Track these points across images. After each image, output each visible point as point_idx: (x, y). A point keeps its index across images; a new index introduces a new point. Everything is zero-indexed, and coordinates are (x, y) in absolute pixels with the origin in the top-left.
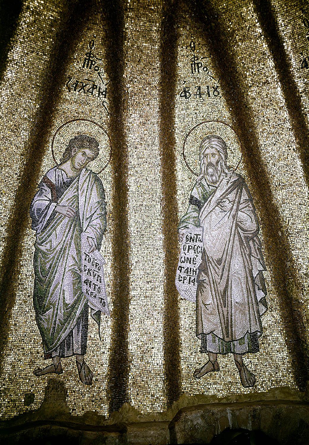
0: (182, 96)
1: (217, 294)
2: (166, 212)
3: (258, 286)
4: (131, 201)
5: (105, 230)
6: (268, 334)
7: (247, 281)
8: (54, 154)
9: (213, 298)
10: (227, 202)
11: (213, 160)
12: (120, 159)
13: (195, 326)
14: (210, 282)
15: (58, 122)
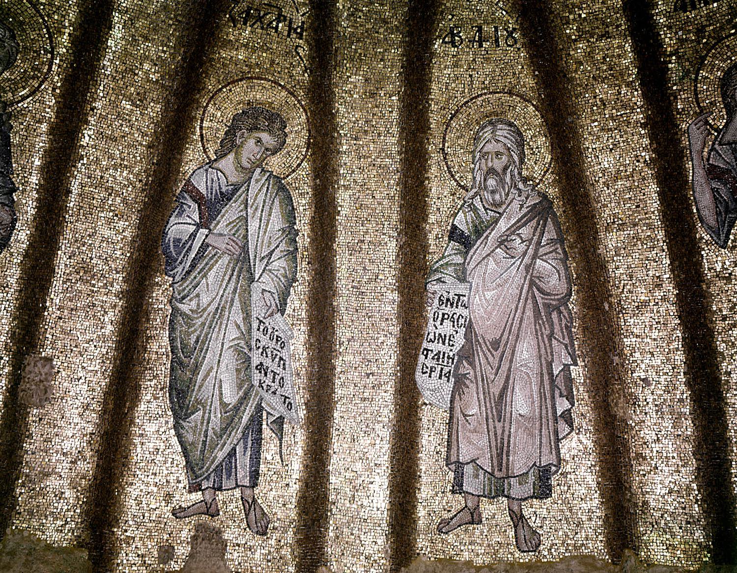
0: (446, 43)
1: (487, 399)
2: (406, 254)
3: (560, 389)
4: (343, 232)
5: (295, 280)
6: (570, 470)
7: (542, 381)
8: (205, 141)
9: (480, 405)
10: (519, 241)
11: (498, 164)
12: (324, 156)
13: (446, 449)
14: (476, 378)
15: (211, 85)
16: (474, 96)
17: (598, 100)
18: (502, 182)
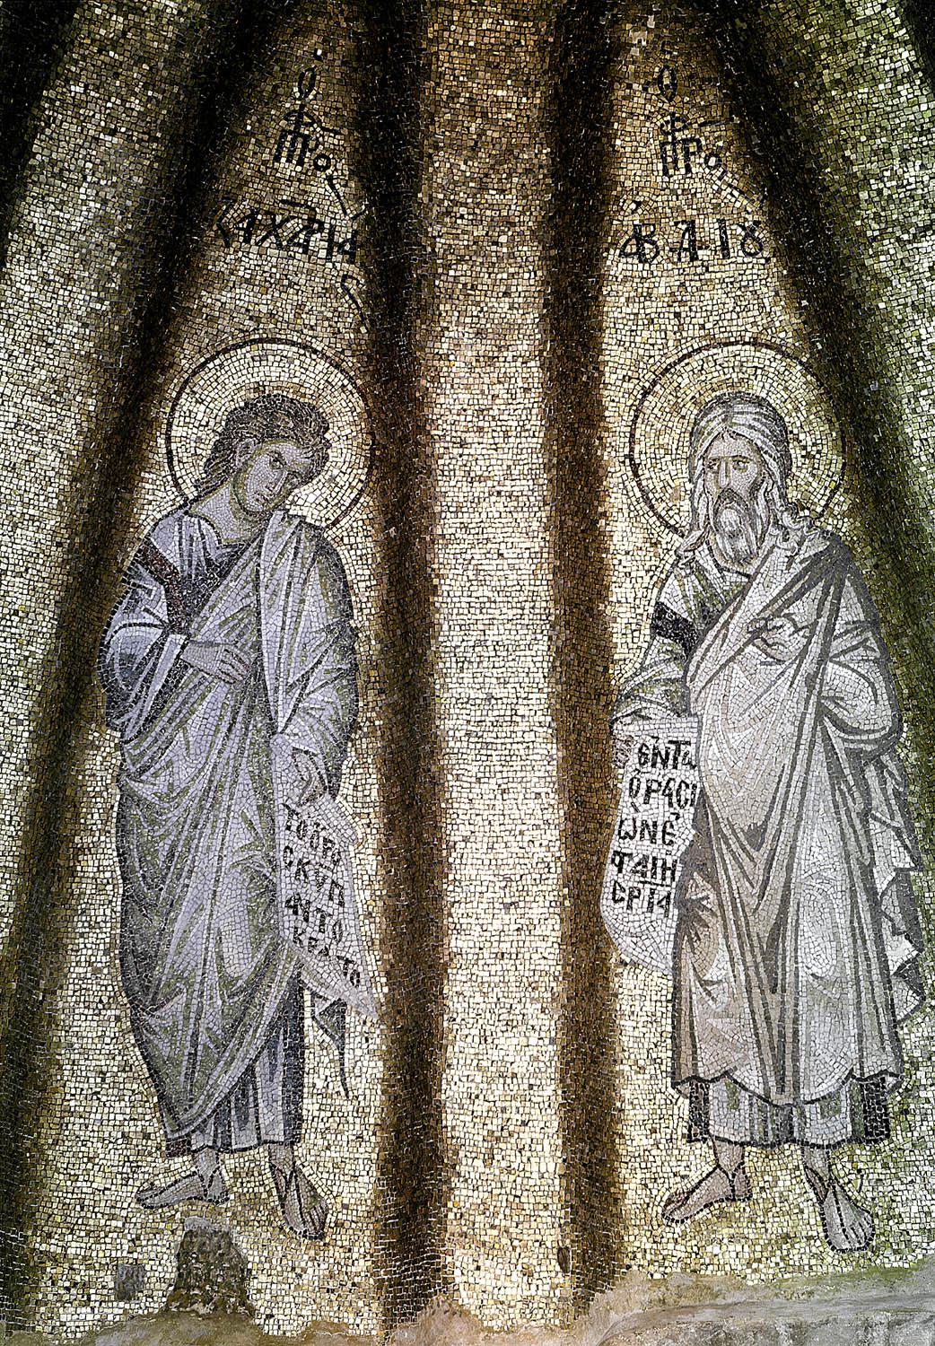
0: (627, 255)
1: (747, 948)
2: (568, 665)
3: (891, 920)
4: (445, 627)
5: (355, 726)
6: (924, 1082)
7: (854, 904)
8: (175, 463)
9: (732, 959)
10: (789, 628)
11: (739, 481)
12: (403, 481)
13: (670, 1054)
14: (721, 906)
15: (186, 357)
16: (685, 352)
17: (925, 348)
18: (751, 514)
